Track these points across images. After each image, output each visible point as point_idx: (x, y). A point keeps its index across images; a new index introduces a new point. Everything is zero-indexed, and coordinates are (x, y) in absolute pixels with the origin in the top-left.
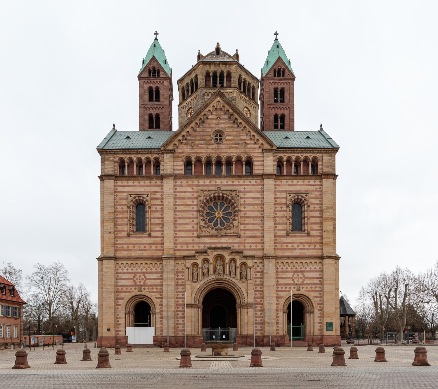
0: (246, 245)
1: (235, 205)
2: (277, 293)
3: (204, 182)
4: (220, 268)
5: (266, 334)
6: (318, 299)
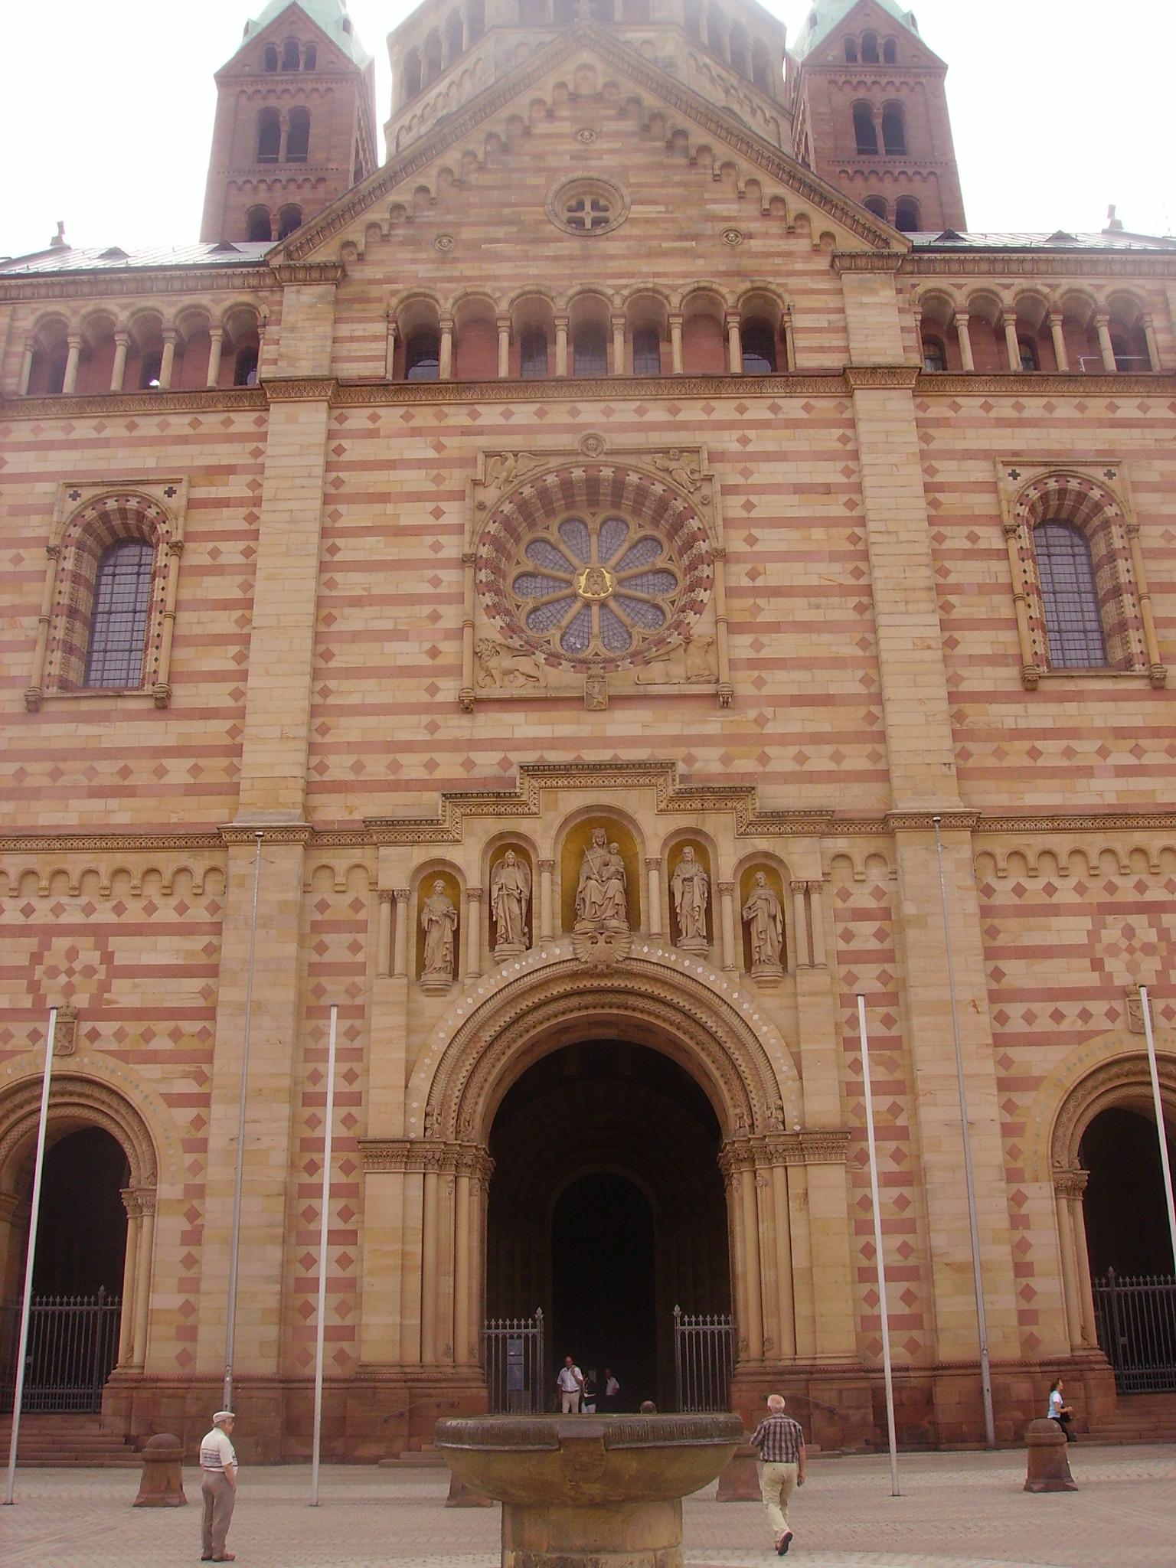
0: (770, 750)
1: (694, 524)
2: (1002, 1050)
5: (947, 1352)
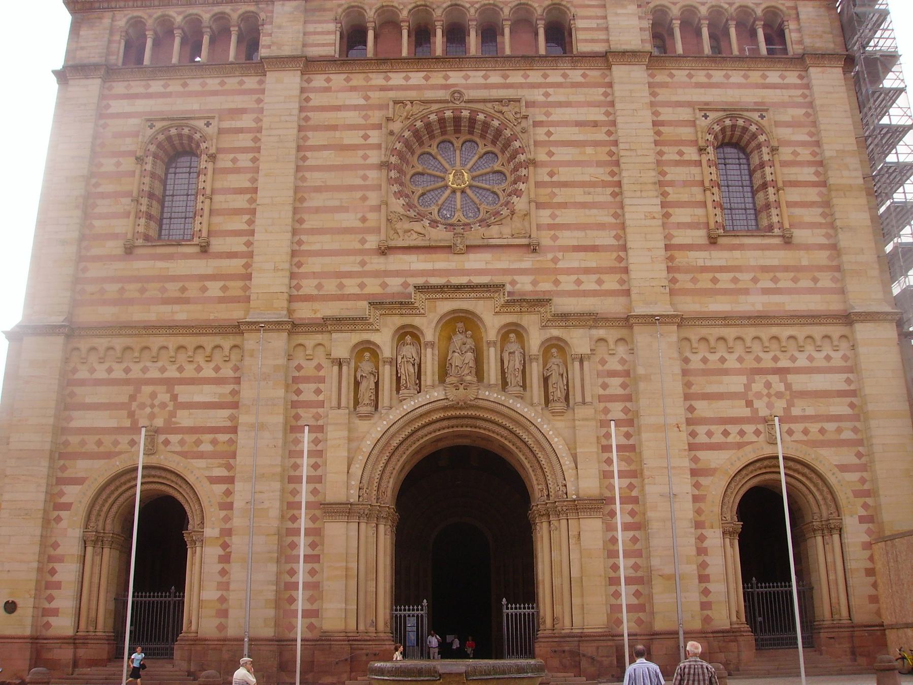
0: (561, 278)
1: (517, 144)
2: (694, 453)
3: (407, 78)
4: (462, 360)
5: (659, 625)
6: (852, 477)
